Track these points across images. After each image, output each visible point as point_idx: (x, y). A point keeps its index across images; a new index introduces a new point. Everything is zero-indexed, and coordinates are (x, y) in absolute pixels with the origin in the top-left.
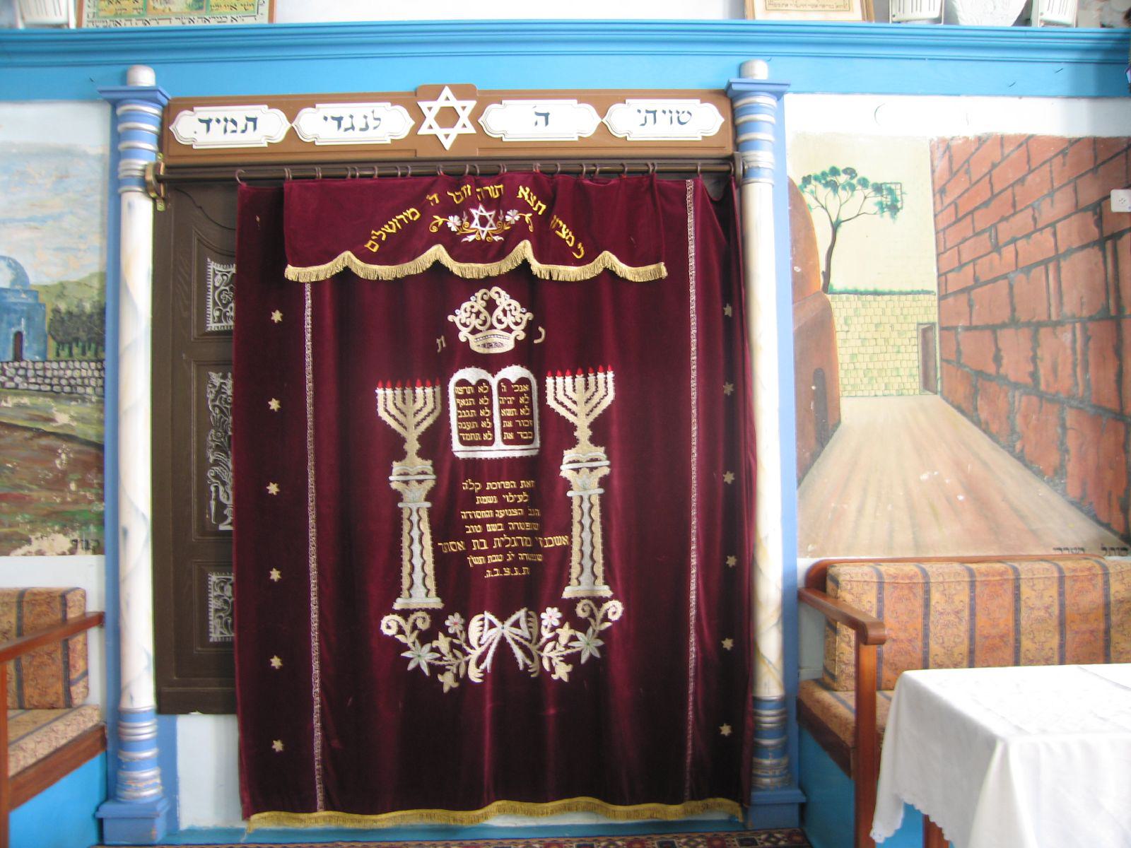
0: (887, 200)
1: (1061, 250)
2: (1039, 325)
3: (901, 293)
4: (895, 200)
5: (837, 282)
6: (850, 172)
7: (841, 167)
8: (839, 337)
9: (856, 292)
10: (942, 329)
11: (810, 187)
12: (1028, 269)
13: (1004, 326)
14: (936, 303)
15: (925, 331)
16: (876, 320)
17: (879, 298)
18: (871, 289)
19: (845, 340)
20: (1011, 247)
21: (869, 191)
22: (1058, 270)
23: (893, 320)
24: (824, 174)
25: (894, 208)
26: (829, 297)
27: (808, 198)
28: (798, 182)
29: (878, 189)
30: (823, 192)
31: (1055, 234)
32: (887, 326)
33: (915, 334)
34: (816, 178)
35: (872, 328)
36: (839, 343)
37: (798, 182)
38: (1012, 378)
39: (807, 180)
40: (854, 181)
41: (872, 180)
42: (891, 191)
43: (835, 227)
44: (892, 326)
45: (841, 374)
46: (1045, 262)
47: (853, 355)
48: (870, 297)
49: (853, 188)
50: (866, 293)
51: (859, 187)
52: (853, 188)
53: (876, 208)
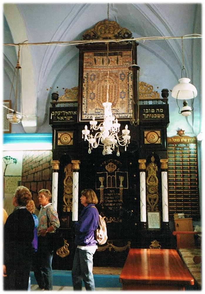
0: (15, 161)
1: (43, 169)
2: (38, 181)
3: (14, 176)
4: (16, 161)
5: (6, 174)
6: (10, 157)
7: (8, 156)
8: (5, 183)
9: (9, 176)
10: (22, 182)
11: (3, 159)
12: (37, 172)
13: (32, 182)
14: (21, 178)
15: (19, 183)
16: (11, 181)
17: (12, 177)
18: (11, 175)
19: (6, 184)
20: (34, 168)
21: (12, 160)
22: (42, 172)
23: (14, 180)
24: (6, 157)
25: (16, 162)
26: (4, 177)
27: (3, 161)
28: (1, 158)
29: (14, 159)
30: (5, 160)
31: (42, 166)
32: (13, 182)
33: (17, 183)
34: (4, 158)
35: (11, 182)
36: (5, 184)
37: (1, 158)
38: (33, 190)
39: (3, 158)
40: (10, 158)
41: (13, 158)
42: (16, 160)
43: (7, 165)
44: (14, 182)
45: (5, 189)
46: (40, 171)
47: (7, 186)
48: (11, 177)
49: (10, 159)
50: (10, 176)
51: (11, 159)
52: (10, 159)
53: (13, 162)
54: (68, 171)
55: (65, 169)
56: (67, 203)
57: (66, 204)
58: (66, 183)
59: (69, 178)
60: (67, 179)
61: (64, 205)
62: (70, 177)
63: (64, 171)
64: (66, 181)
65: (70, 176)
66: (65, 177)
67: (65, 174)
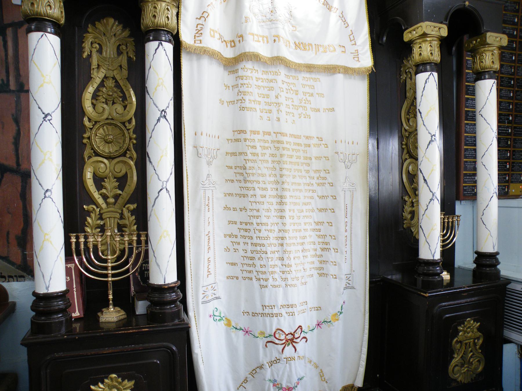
54: (100, 51)
55: (87, 46)
56: (105, 197)
57: (100, 201)
58: (94, 105)
59: (110, 83)
60: (97, 90)
61: (88, 205)
62: (114, 78)
63: (81, 50)
64: (95, 96)
65: (110, 74)
66: (90, 78)
67: (90, 65)
